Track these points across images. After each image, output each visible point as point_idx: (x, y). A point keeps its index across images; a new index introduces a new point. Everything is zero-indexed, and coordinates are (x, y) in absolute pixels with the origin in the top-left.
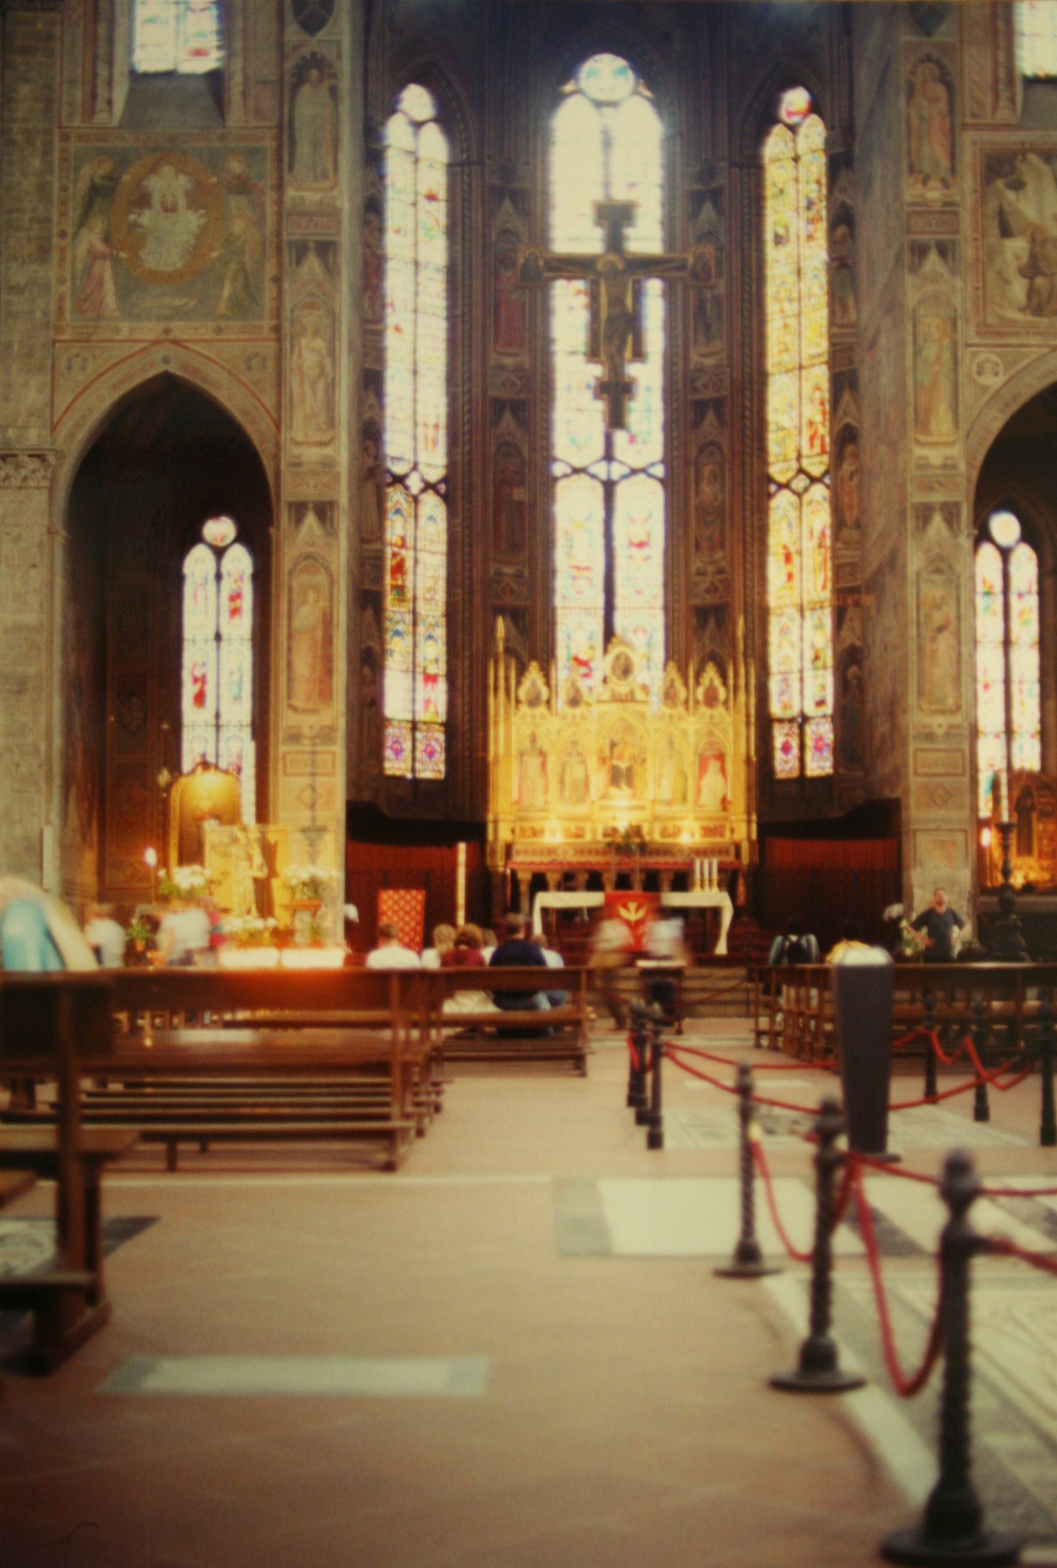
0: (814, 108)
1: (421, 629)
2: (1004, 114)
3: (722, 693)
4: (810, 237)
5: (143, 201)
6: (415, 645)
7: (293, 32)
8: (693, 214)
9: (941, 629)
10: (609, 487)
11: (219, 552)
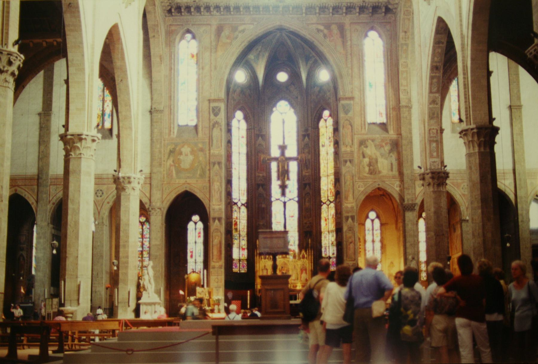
0: (330, 115)
1: (241, 238)
2: (363, 131)
3: (306, 256)
4: (330, 146)
5: (181, 153)
6: (240, 242)
7: (212, 116)
8: (303, 140)
9: (351, 243)
10: (285, 203)
11: (196, 223)
